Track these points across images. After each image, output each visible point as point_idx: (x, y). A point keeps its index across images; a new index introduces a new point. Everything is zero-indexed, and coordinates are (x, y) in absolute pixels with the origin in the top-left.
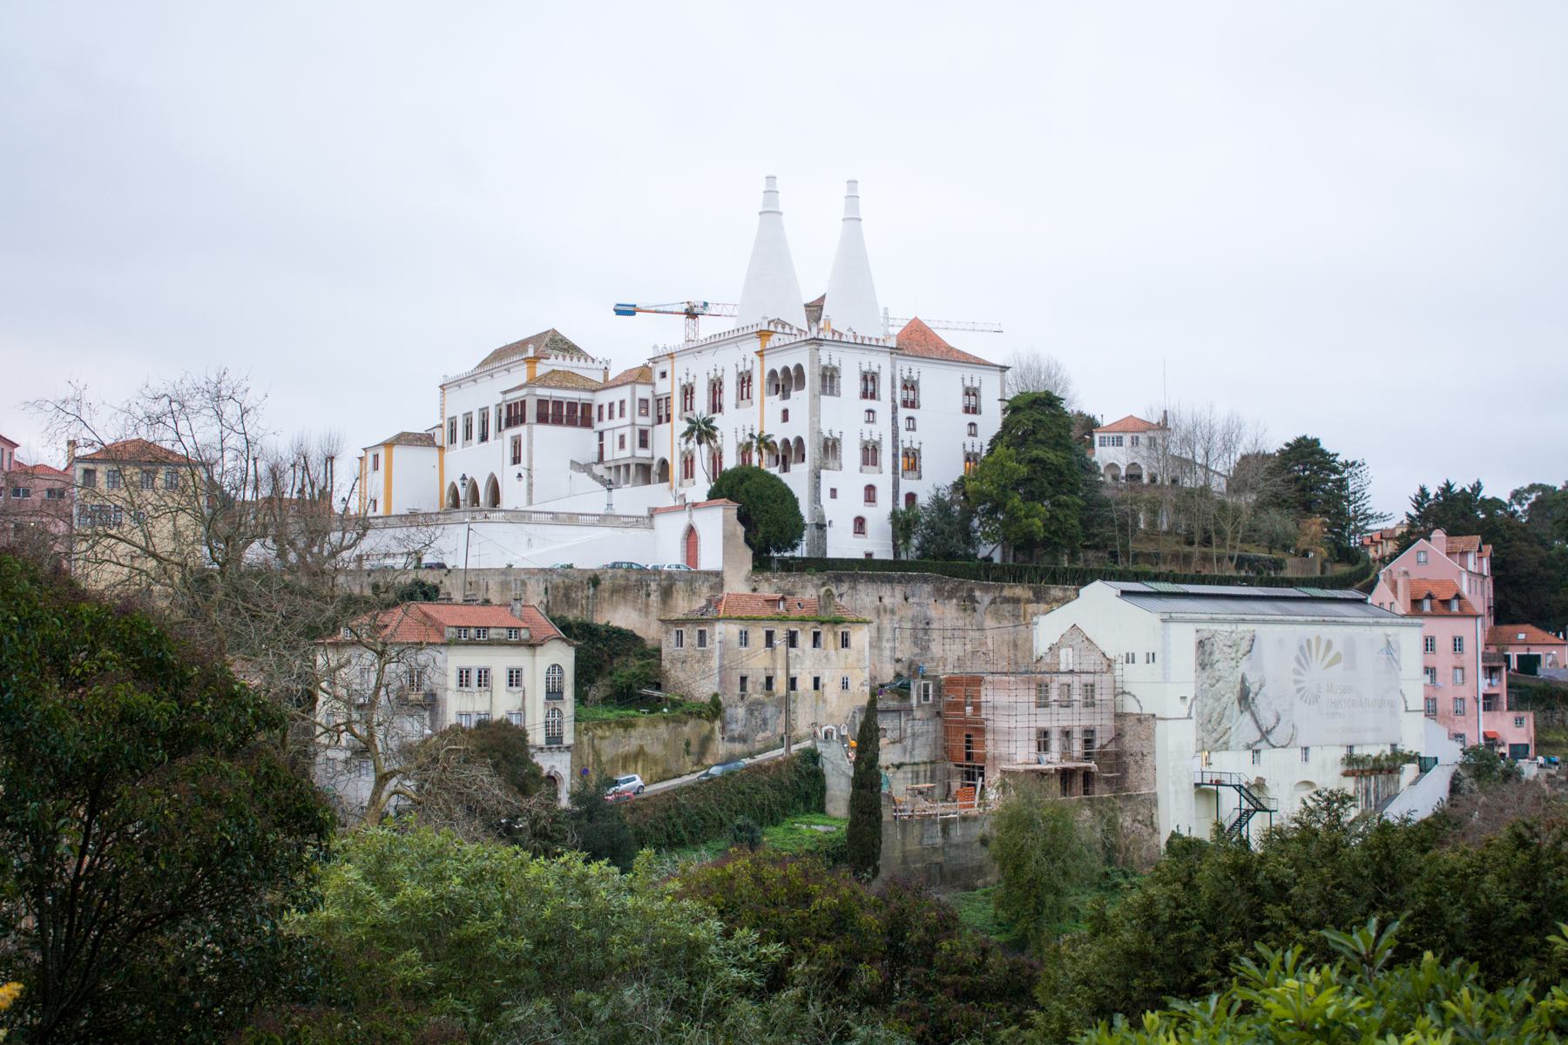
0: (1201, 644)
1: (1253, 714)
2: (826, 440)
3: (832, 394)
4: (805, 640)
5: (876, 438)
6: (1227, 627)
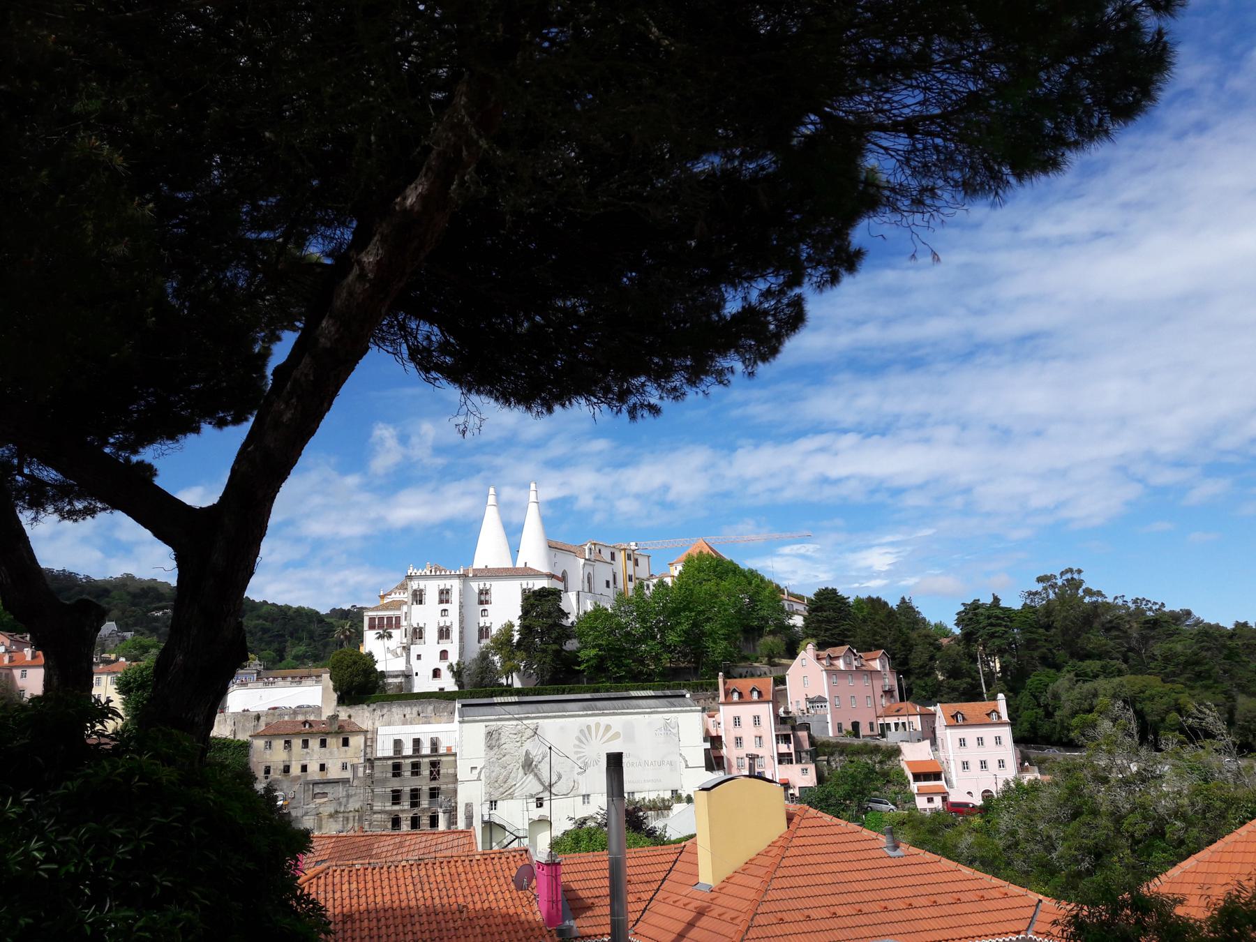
0: (490, 734)
1: (536, 775)
2: (415, 629)
3: (421, 602)
4: (314, 743)
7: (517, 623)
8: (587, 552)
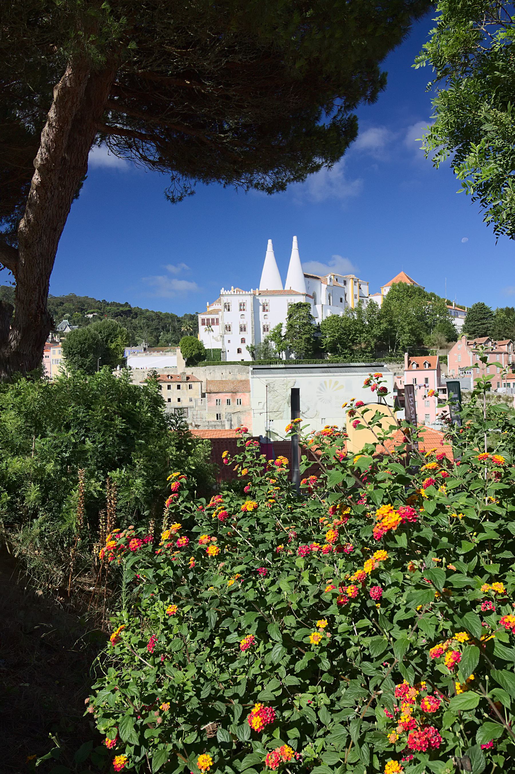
5: (245, 323)
6: (283, 379)
7: (285, 324)
8: (328, 280)
